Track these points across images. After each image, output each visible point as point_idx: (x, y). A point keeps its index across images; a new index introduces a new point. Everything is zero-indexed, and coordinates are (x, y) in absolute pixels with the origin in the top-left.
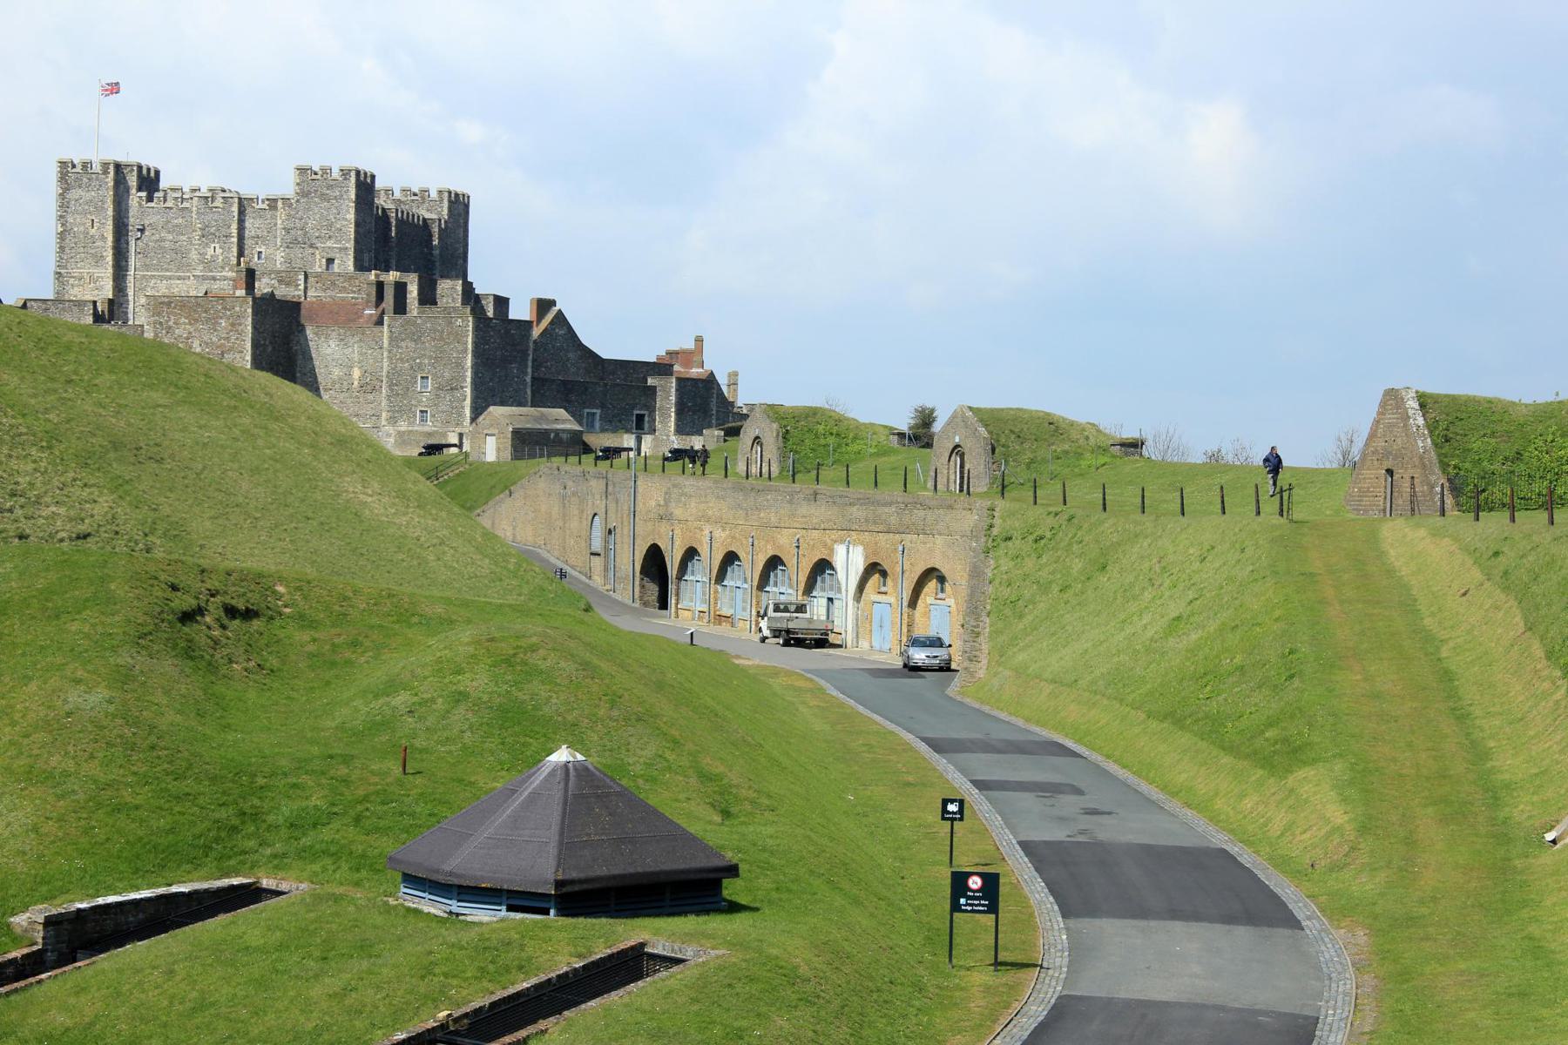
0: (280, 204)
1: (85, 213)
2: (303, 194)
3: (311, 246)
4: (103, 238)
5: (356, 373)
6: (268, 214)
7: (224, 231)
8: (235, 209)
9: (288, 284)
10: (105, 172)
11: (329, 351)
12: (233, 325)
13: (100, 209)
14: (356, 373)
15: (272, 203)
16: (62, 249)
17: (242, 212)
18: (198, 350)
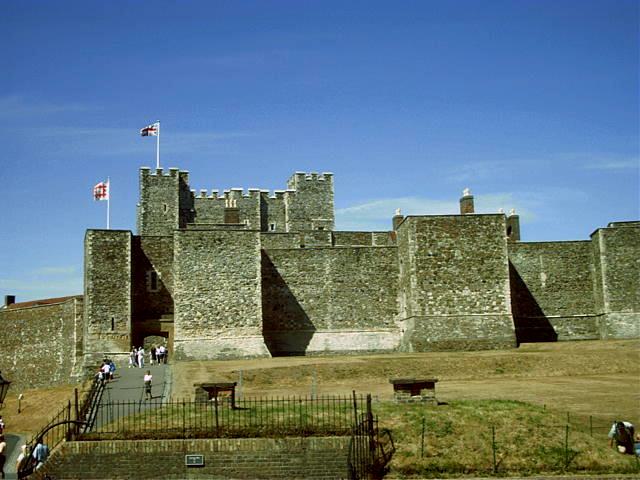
0: (286, 196)
1: (160, 201)
2: (302, 188)
3: (309, 220)
4: (173, 217)
5: (543, 277)
6: (277, 202)
7: (252, 212)
8: (258, 198)
9: (321, 239)
10: (174, 176)
11: (518, 261)
12: (490, 237)
13: (170, 199)
14: (543, 277)
15: (280, 196)
16: (145, 224)
17: (264, 204)
18: (461, 258)
